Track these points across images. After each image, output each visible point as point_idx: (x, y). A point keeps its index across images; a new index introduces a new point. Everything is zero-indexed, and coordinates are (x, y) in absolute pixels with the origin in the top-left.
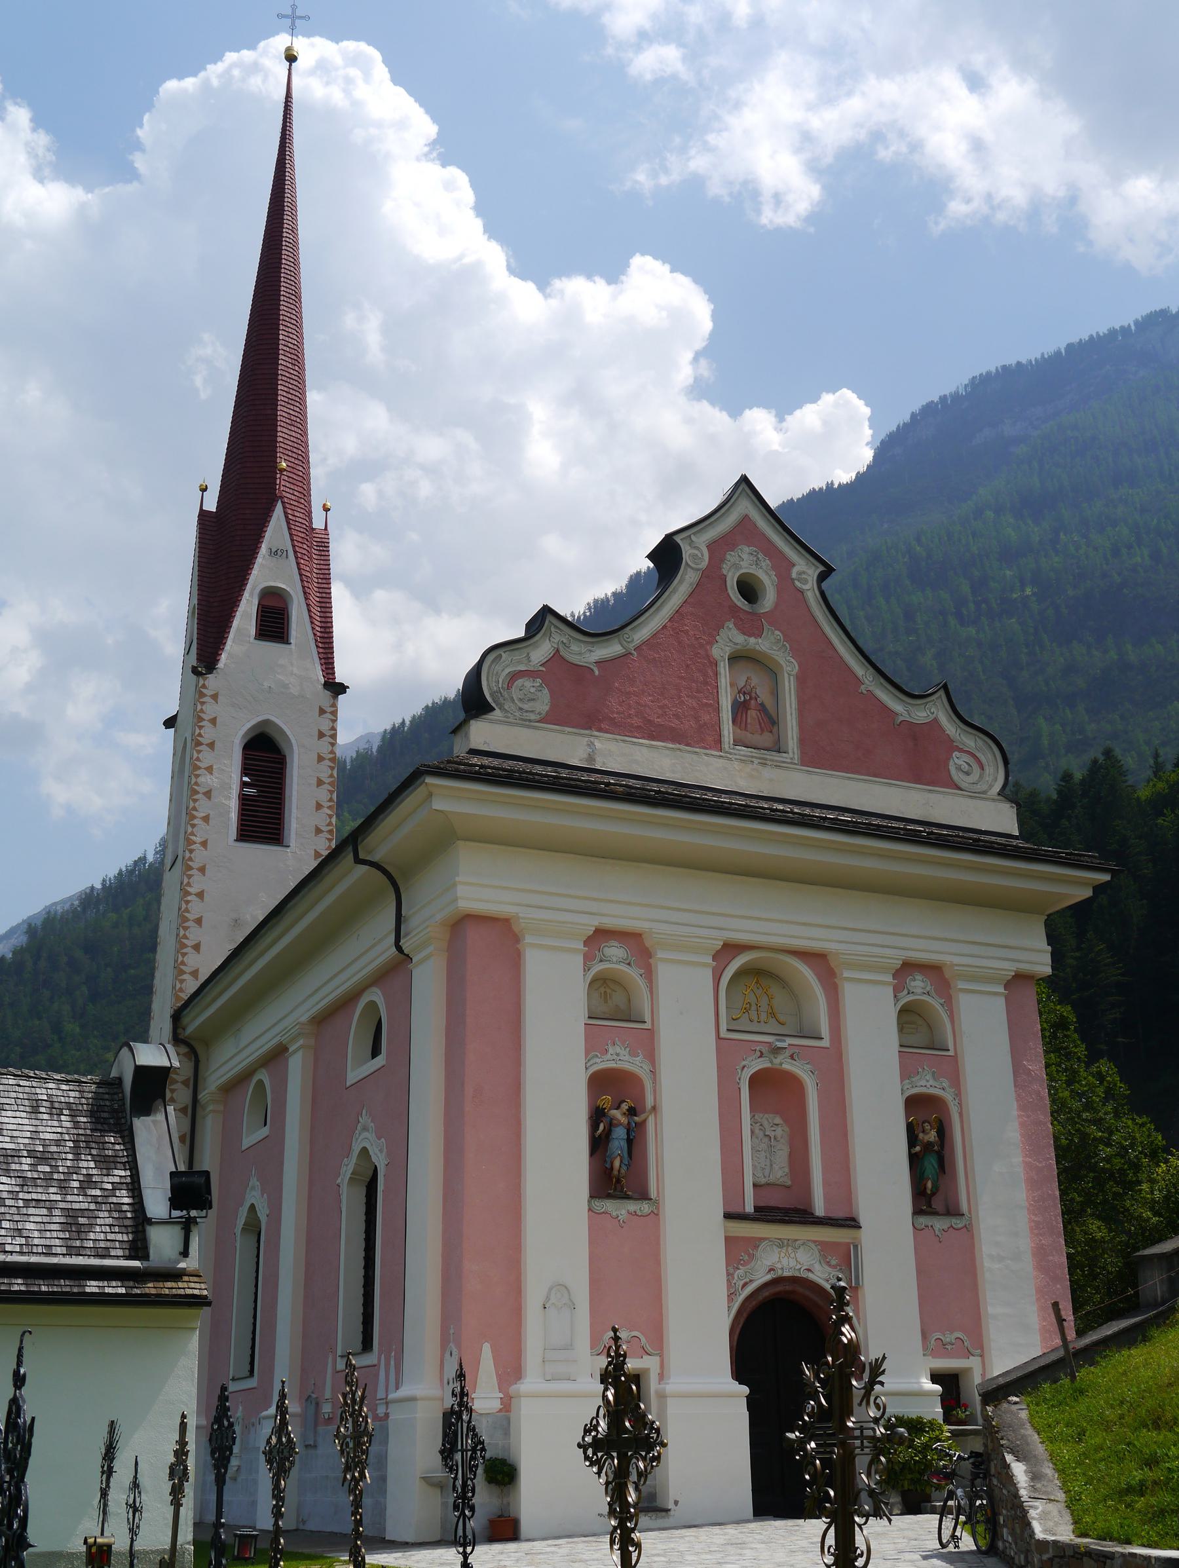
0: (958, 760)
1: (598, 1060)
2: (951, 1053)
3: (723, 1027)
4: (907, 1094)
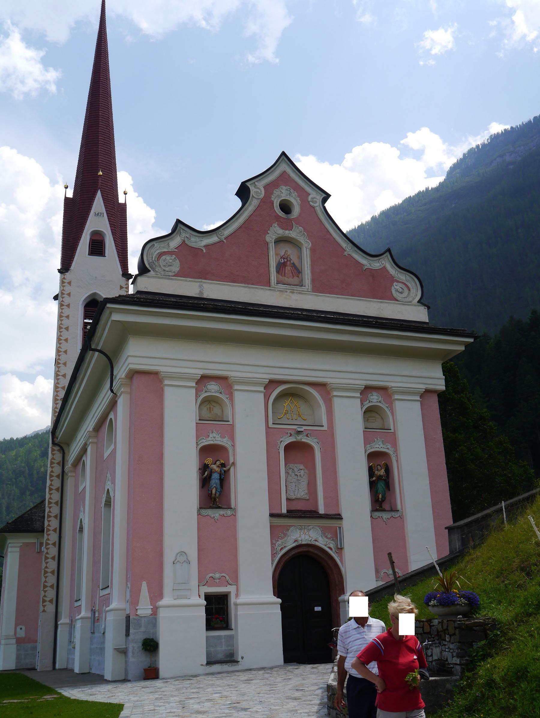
0: (396, 286)
1: (204, 441)
2: (392, 431)
3: (271, 421)
4: (368, 452)
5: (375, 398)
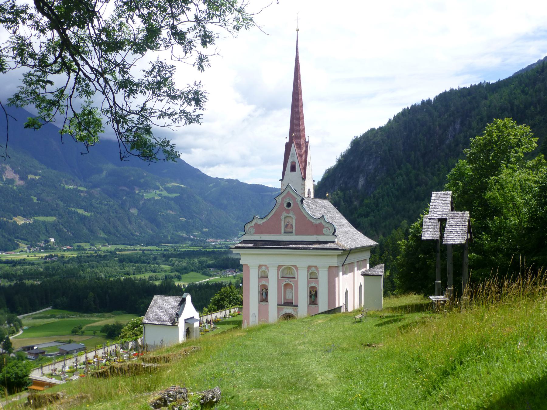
0: (325, 229)
5: (313, 270)
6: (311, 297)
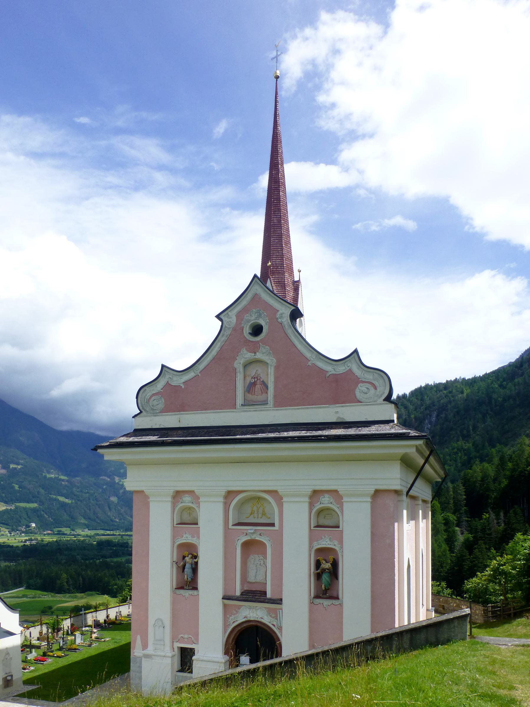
0: (362, 387)
5: (326, 501)
6: (318, 577)
